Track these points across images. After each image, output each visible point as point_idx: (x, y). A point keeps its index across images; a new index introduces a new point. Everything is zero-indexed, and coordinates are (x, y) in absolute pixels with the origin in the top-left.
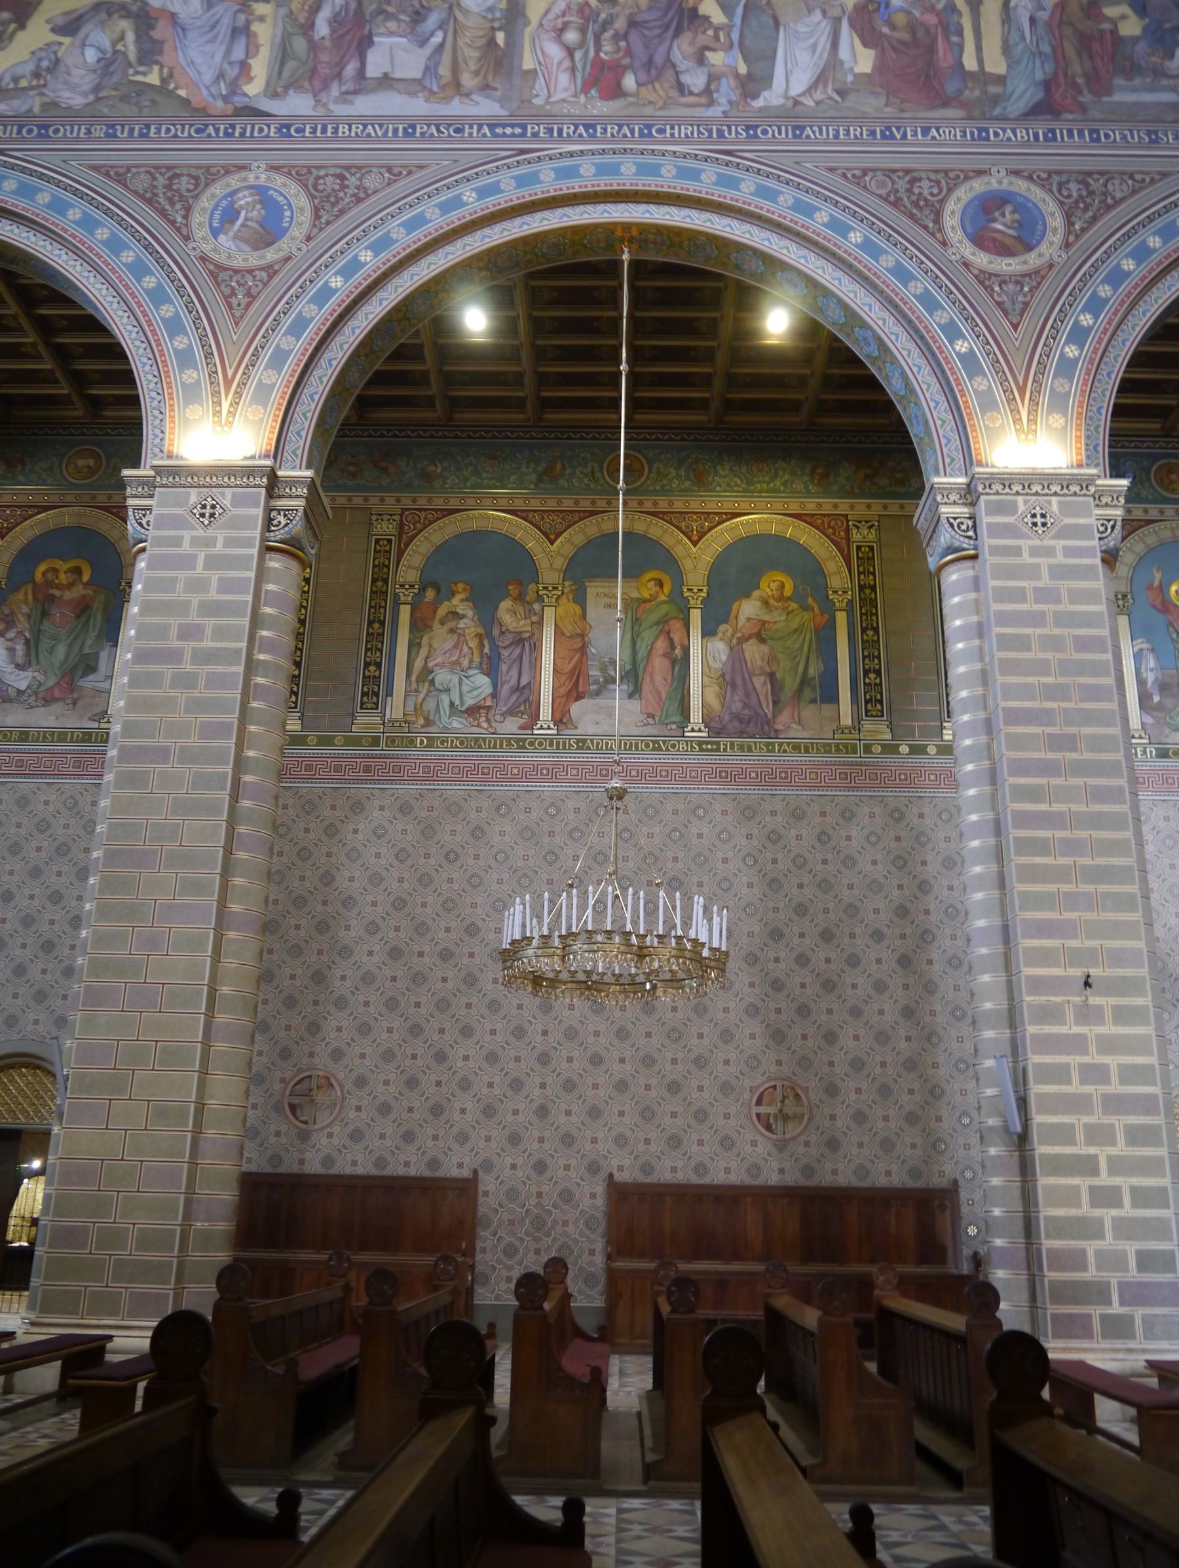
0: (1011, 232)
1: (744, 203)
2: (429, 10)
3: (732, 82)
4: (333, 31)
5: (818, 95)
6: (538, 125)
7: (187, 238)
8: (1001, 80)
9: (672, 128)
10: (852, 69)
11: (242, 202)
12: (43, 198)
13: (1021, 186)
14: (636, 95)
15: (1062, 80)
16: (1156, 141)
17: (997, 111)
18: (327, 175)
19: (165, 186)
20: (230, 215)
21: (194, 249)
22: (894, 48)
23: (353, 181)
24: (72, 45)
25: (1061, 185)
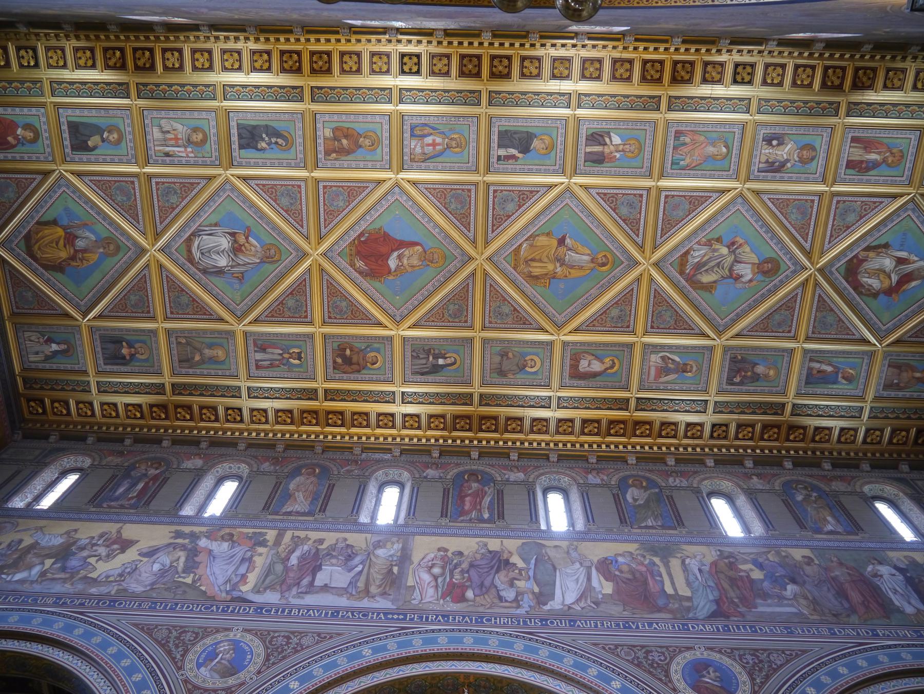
0: (716, 683)
1: (542, 662)
2: (357, 555)
3: (531, 596)
4: (299, 562)
5: (582, 604)
6: (414, 614)
7: (179, 668)
8: (689, 599)
9: (496, 619)
10: (601, 591)
11: (222, 649)
12: (97, 640)
13: (716, 656)
14: (474, 601)
15: (725, 600)
16: (792, 632)
17: (691, 615)
18: (279, 636)
19: (176, 637)
20: (212, 655)
21: (182, 675)
22: (623, 582)
23: (295, 640)
24: (148, 561)
25: (740, 656)
